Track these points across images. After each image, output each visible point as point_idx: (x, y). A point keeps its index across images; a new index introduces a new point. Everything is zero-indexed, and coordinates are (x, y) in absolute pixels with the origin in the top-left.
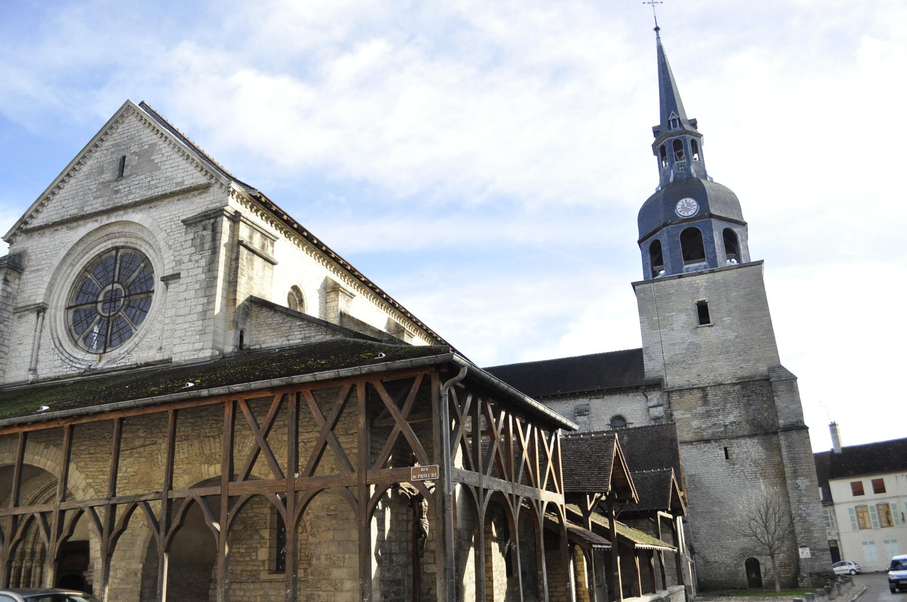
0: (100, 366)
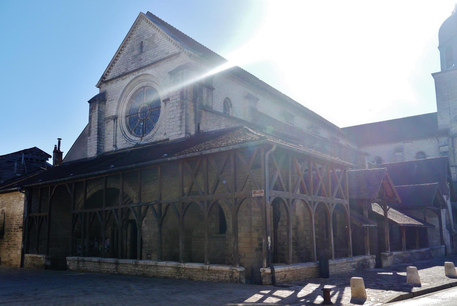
0: (141, 143)
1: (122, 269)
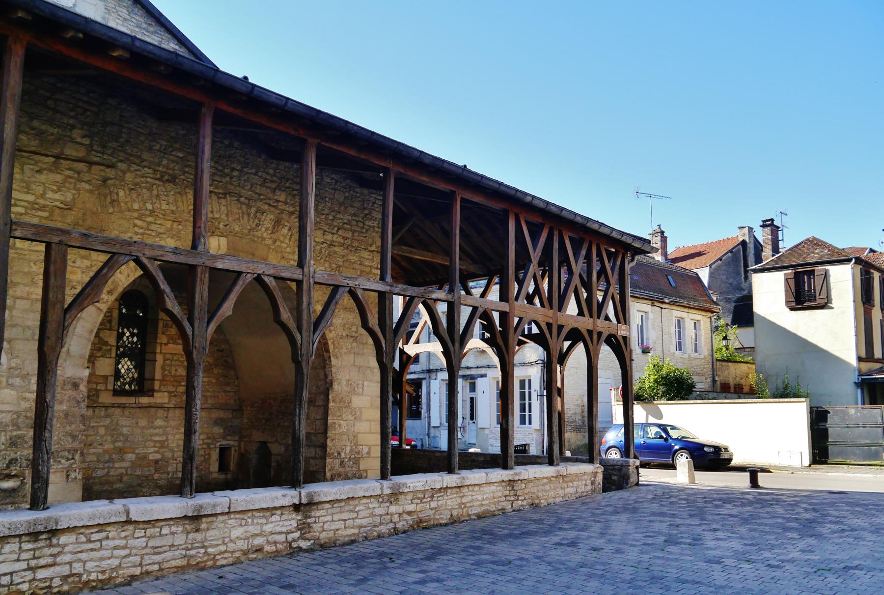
1: (330, 524)
